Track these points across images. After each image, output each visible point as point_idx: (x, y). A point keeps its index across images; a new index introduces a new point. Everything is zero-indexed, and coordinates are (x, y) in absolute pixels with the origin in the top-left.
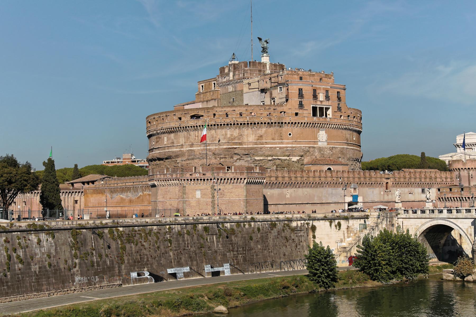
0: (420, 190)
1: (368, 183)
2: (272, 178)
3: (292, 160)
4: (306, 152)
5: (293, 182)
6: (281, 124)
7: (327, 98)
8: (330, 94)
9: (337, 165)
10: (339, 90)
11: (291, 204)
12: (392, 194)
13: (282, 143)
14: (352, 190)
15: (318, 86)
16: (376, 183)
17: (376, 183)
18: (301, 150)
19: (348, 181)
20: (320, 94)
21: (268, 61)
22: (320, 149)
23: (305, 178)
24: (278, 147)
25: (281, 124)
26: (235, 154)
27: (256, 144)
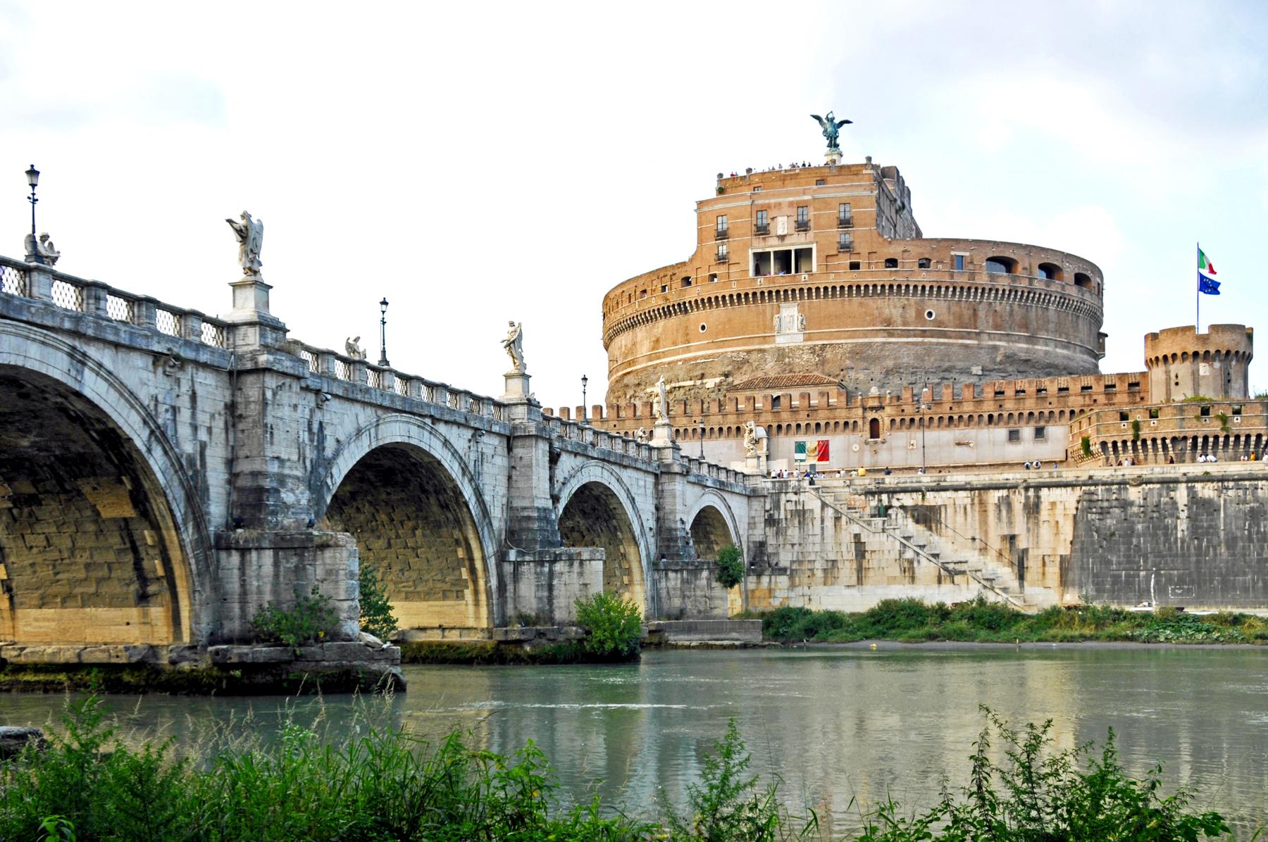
0: (1001, 433)
1: (803, 424)
4: (740, 364)
6: (683, 308)
7: (802, 226)
8: (810, 214)
12: (890, 449)
13: (688, 350)
15: (773, 201)
16: (832, 423)
17: (832, 423)
18: (726, 361)
22: (781, 354)
23: (612, 424)
25: (683, 308)
26: (627, 386)
27: (650, 358)
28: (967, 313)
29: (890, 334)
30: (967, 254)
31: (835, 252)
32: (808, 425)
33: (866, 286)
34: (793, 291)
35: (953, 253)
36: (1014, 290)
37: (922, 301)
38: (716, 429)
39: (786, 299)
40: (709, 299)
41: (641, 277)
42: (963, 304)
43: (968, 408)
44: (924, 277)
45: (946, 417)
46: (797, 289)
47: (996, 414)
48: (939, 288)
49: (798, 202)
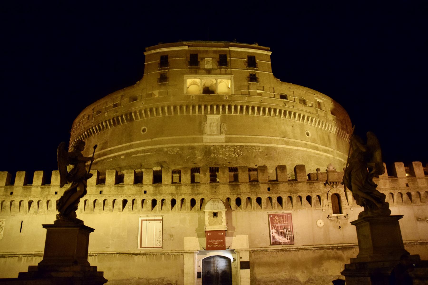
13: (131, 147)
14: (207, 217)
19: (193, 193)
24: (123, 155)
28: (326, 137)
29: (287, 143)
30: (322, 101)
34: (218, 107)
35: (316, 98)
39: (212, 112)
45: (404, 192)
49: (219, 51)
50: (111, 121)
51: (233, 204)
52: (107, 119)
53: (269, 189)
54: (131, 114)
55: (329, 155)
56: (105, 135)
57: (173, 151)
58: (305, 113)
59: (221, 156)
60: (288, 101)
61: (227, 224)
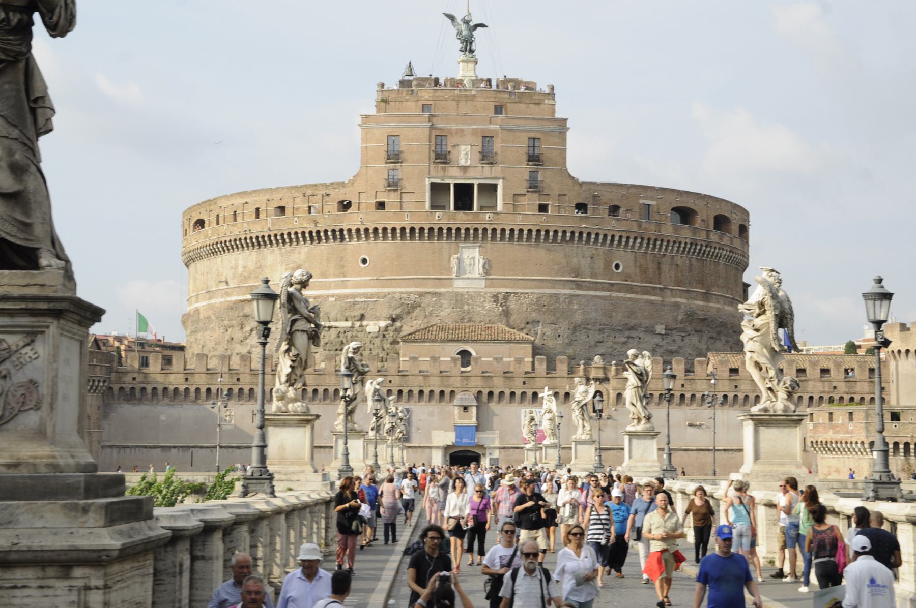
1: (518, 393)
2: (172, 378)
3: (369, 329)
4: (410, 308)
5: (246, 389)
6: (339, 235)
7: (487, 157)
8: (497, 146)
9: (493, 341)
10: (533, 135)
11: (239, 448)
13: (344, 285)
14: (457, 411)
15: (454, 126)
20: (463, 148)
21: (472, 73)
22: (459, 299)
24: (333, 296)
25: (339, 235)
26: (246, 316)
28: (652, 267)
29: (579, 285)
30: (653, 203)
31: (524, 191)
32: (524, 393)
33: (556, 232)
34: (476, 230)
35: (641, 201)
36: (694, 243)
37: (610, 251)
38: (416, 391)
39: (467, 237)
40: (376, 230)
41: (277, 189)
42: (648, 256)
43: (701, 387)
44: (612, 225)
46: (480, 228)
47: (731, 396)
48: (628, 238)
49: (483, 130)
50: (307, 235)
51: (485, 397)
52: (300, 231)
53: (524, 383)
54: (341, 231)
55: (653, 298)
56: (296, 256)
57: (409, 299)
58: (614, 233)
59: (478, 309)
60: (588, 215)
61: (478, 418)
